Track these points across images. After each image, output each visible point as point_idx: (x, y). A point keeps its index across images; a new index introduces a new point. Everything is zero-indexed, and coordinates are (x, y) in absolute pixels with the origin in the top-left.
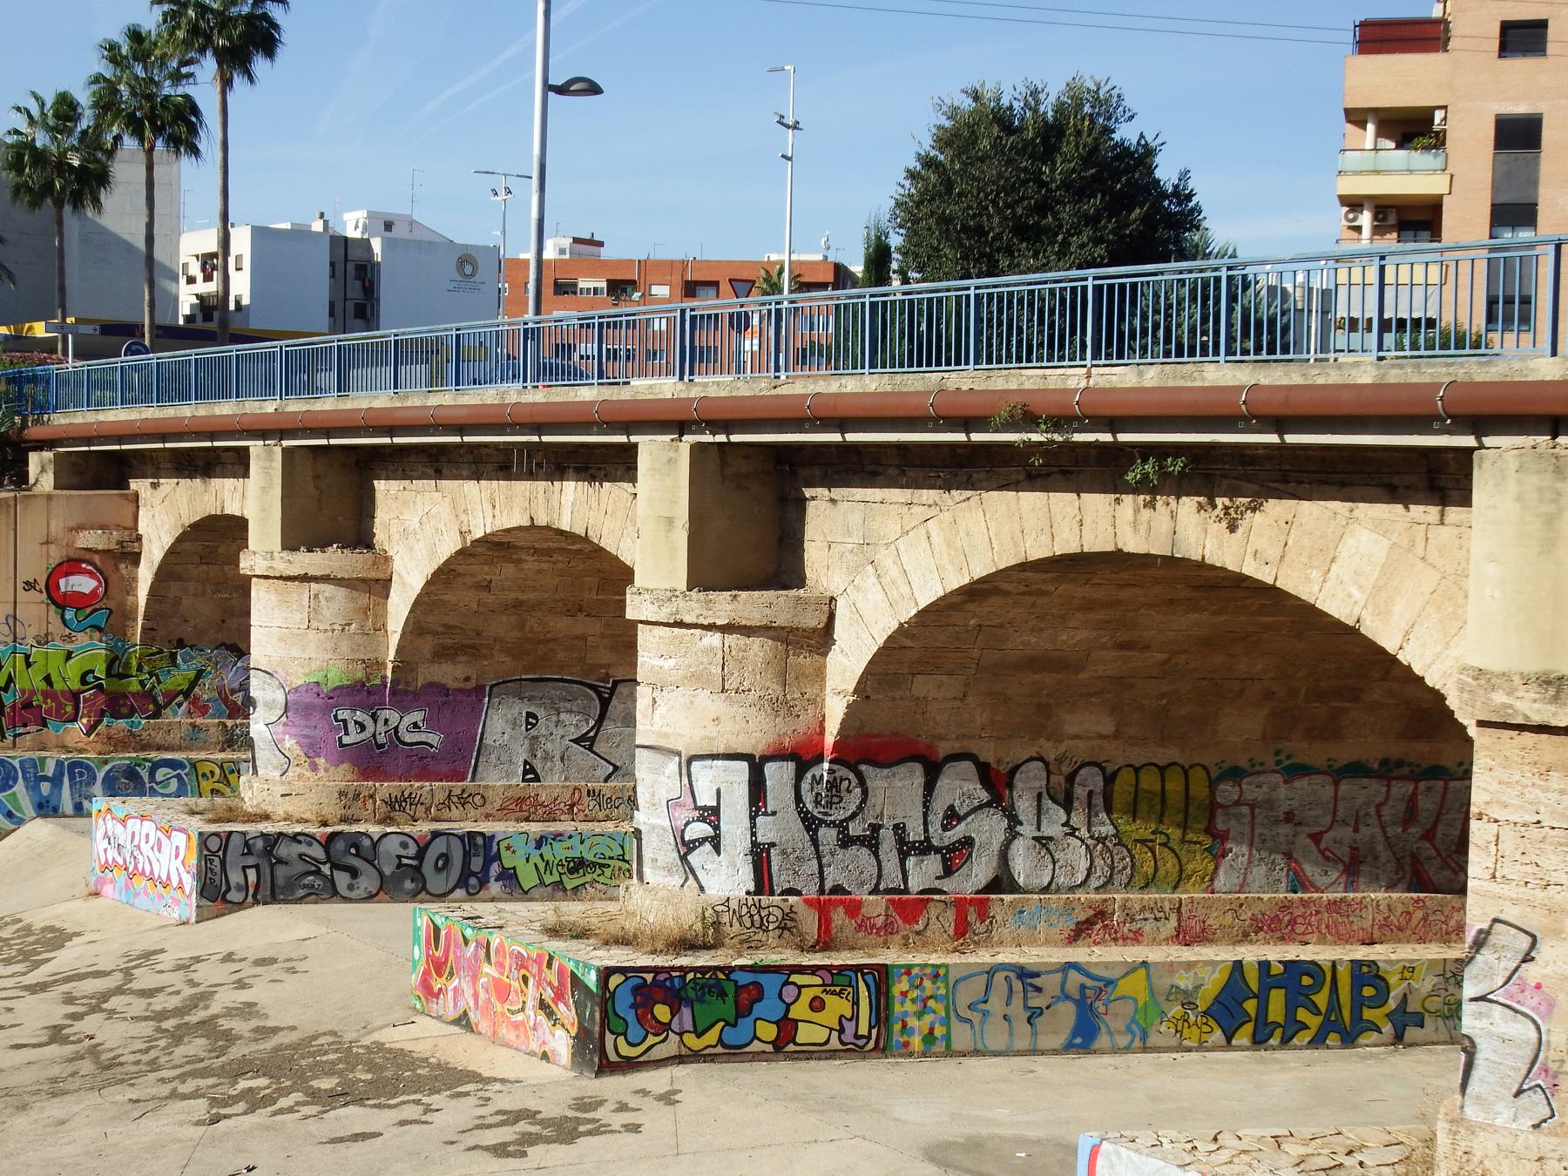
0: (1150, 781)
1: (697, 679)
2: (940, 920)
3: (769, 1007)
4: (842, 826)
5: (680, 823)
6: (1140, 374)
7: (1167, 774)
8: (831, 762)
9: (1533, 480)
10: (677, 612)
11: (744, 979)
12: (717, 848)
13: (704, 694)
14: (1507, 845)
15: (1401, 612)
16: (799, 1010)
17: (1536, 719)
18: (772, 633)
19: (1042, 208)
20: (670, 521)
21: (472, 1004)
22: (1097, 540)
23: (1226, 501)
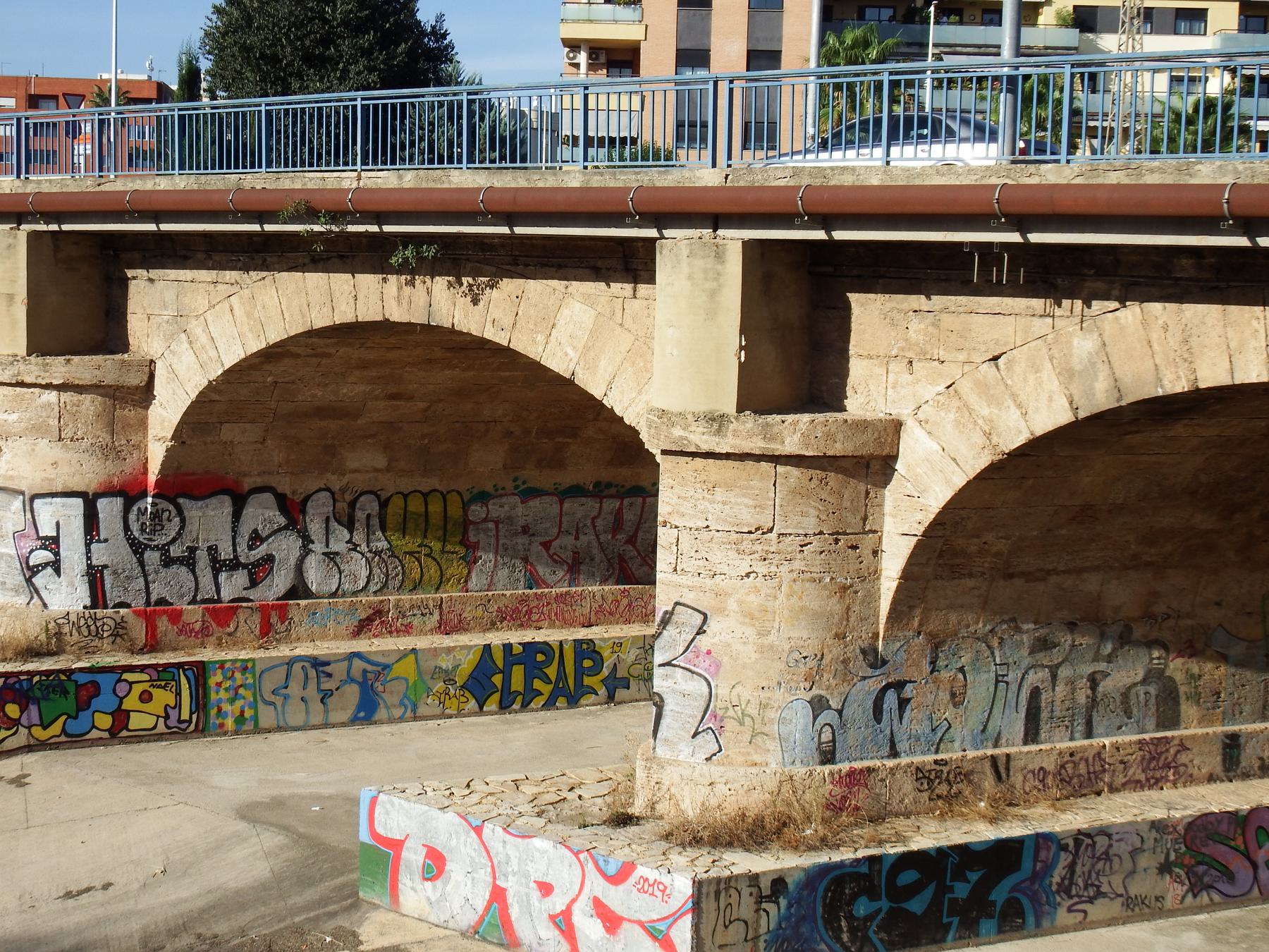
0: (416, 505)
1: (37, 430)
2: (247, 623)
3: (105, 701)
4: (164, 549)
5: (25, 551)
6: (400, 177)
7: (429, 499)
8: (153, 497)
9: (700, 263)
10: (19, 374)
11: (83, 679)
12: (58, 571)
13: (43, 443)
14: (684, 546)
15: (605, 367)
16: (131, 702)
17: (705, 448)
18: (102, 391)
19: (326, 41)
20: (11, 297)
22: (368, 313)
23: (470, 280)
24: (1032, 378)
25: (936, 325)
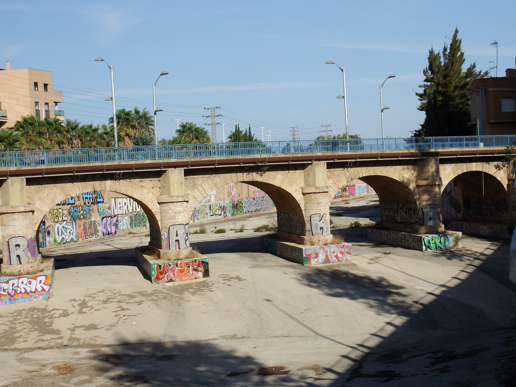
9: (323, 166)
15: (285, 184)
21: (173, 276)
23: (260, 172)
24: (342, 178)
25: (331, 173)
